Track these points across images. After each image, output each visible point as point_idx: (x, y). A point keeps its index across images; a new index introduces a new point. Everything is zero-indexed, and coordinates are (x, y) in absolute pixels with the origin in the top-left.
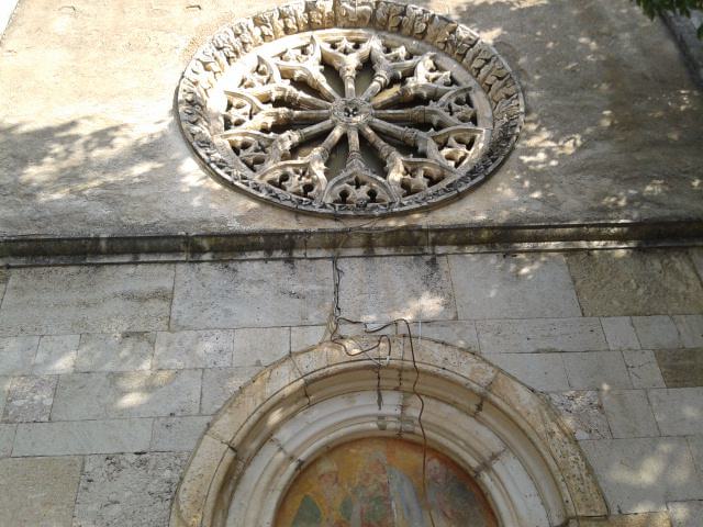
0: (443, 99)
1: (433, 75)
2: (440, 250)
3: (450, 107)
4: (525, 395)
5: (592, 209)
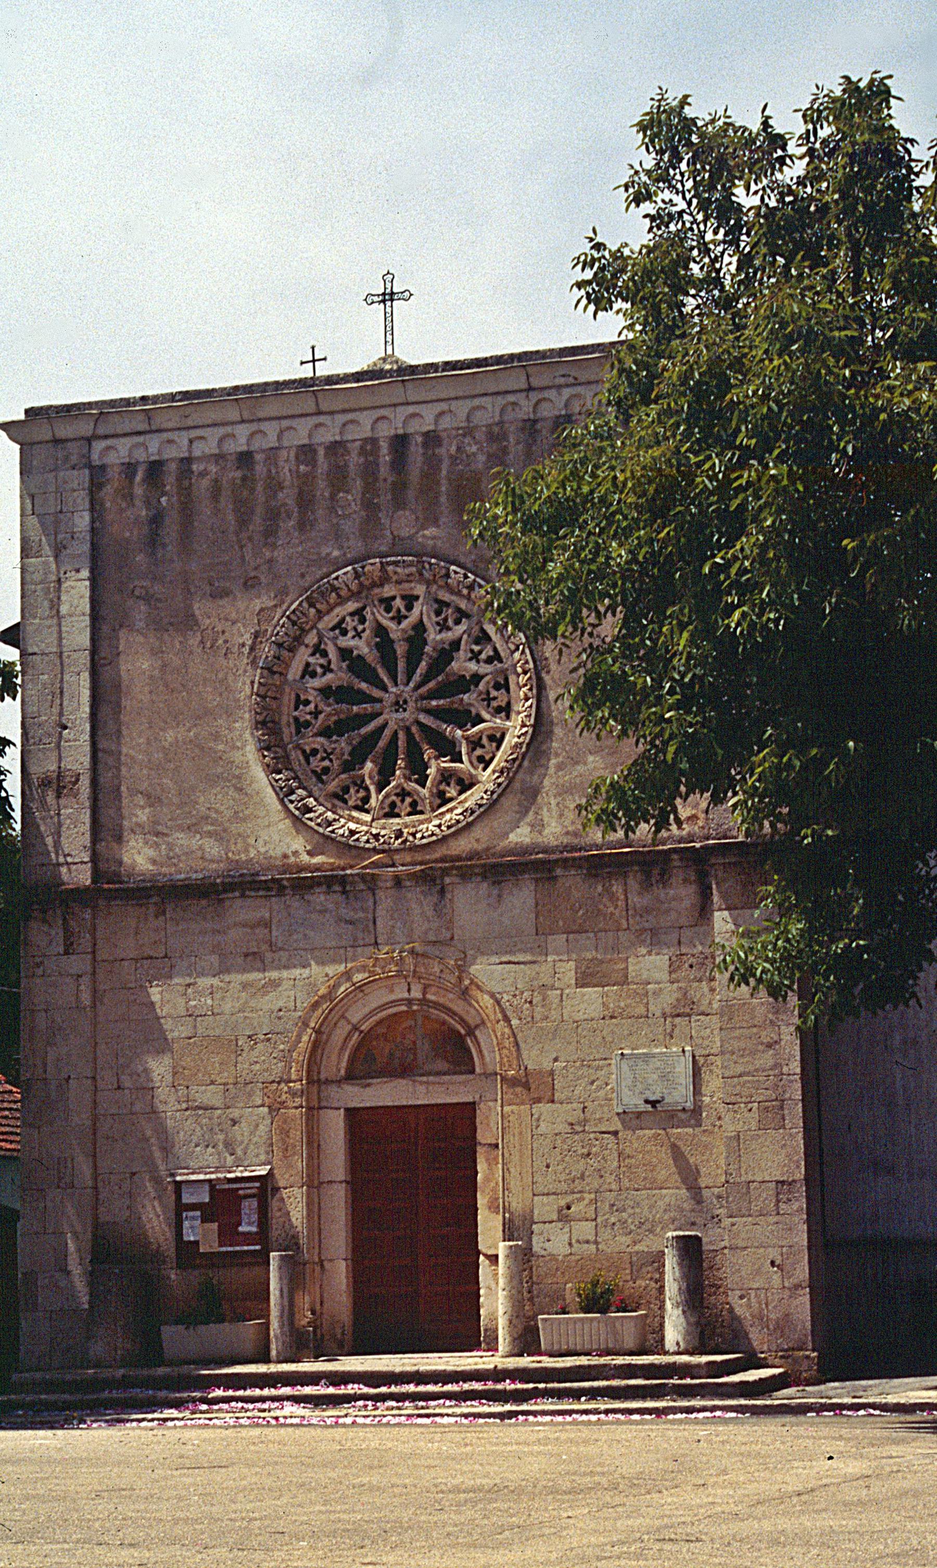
0: (482, 686)
1: (476, 648)
2: (447, 880)
3: (488, 693)
4: (486, 997)
5: (567, 833)
